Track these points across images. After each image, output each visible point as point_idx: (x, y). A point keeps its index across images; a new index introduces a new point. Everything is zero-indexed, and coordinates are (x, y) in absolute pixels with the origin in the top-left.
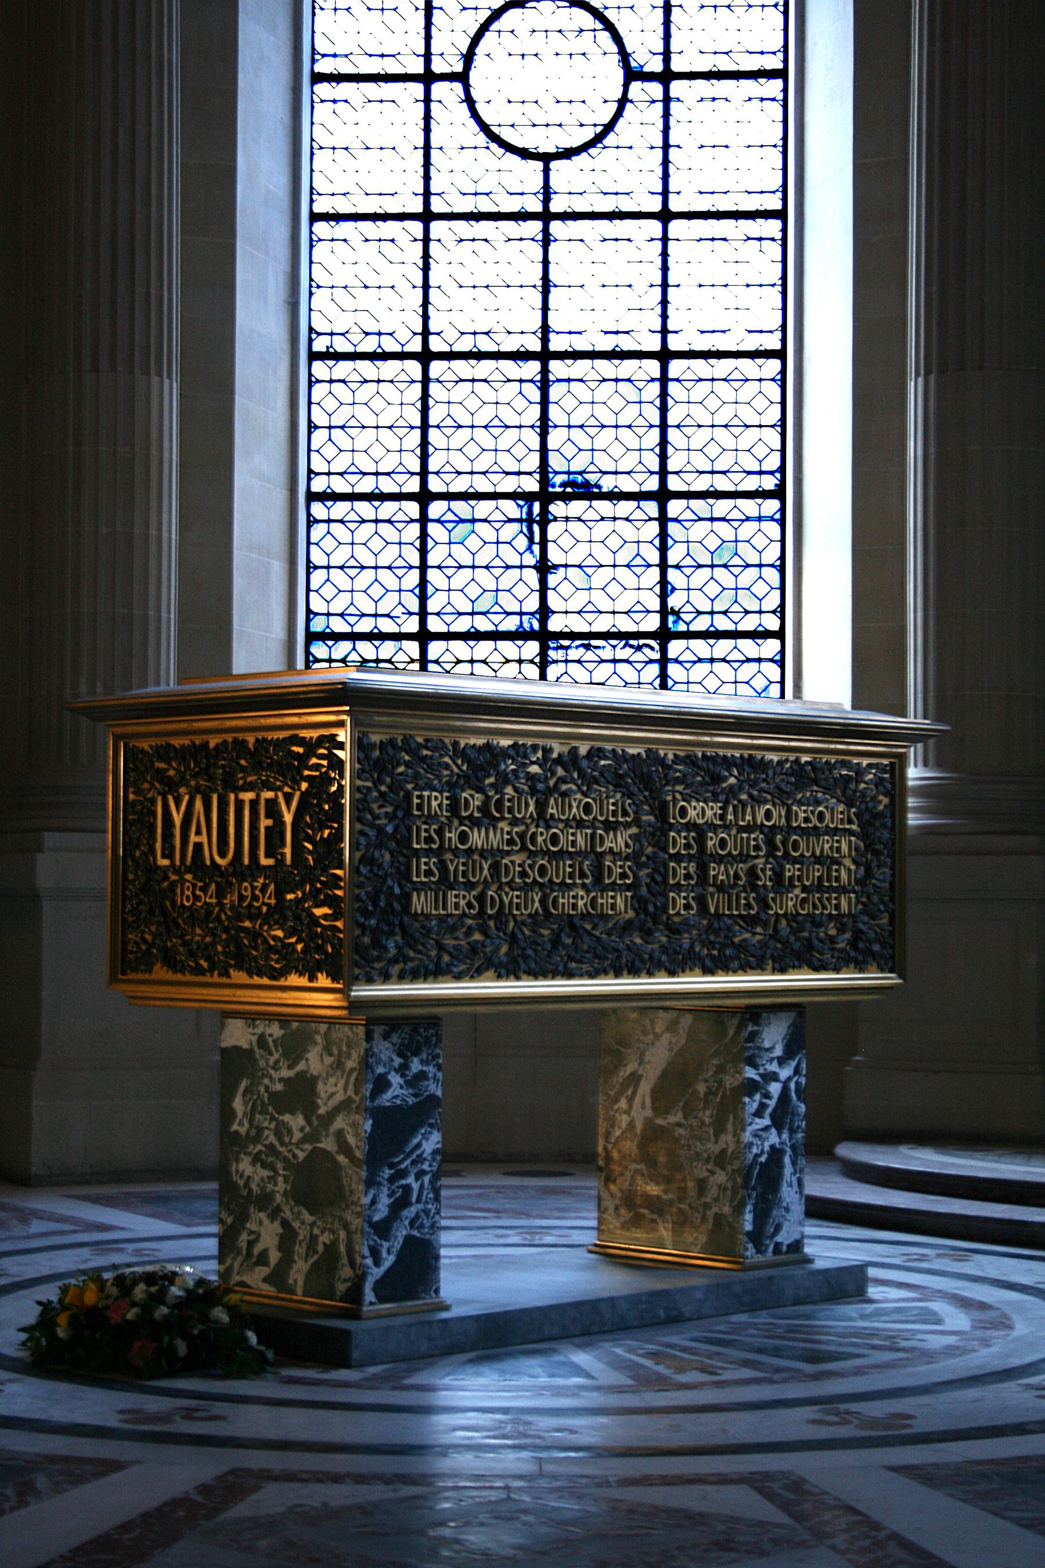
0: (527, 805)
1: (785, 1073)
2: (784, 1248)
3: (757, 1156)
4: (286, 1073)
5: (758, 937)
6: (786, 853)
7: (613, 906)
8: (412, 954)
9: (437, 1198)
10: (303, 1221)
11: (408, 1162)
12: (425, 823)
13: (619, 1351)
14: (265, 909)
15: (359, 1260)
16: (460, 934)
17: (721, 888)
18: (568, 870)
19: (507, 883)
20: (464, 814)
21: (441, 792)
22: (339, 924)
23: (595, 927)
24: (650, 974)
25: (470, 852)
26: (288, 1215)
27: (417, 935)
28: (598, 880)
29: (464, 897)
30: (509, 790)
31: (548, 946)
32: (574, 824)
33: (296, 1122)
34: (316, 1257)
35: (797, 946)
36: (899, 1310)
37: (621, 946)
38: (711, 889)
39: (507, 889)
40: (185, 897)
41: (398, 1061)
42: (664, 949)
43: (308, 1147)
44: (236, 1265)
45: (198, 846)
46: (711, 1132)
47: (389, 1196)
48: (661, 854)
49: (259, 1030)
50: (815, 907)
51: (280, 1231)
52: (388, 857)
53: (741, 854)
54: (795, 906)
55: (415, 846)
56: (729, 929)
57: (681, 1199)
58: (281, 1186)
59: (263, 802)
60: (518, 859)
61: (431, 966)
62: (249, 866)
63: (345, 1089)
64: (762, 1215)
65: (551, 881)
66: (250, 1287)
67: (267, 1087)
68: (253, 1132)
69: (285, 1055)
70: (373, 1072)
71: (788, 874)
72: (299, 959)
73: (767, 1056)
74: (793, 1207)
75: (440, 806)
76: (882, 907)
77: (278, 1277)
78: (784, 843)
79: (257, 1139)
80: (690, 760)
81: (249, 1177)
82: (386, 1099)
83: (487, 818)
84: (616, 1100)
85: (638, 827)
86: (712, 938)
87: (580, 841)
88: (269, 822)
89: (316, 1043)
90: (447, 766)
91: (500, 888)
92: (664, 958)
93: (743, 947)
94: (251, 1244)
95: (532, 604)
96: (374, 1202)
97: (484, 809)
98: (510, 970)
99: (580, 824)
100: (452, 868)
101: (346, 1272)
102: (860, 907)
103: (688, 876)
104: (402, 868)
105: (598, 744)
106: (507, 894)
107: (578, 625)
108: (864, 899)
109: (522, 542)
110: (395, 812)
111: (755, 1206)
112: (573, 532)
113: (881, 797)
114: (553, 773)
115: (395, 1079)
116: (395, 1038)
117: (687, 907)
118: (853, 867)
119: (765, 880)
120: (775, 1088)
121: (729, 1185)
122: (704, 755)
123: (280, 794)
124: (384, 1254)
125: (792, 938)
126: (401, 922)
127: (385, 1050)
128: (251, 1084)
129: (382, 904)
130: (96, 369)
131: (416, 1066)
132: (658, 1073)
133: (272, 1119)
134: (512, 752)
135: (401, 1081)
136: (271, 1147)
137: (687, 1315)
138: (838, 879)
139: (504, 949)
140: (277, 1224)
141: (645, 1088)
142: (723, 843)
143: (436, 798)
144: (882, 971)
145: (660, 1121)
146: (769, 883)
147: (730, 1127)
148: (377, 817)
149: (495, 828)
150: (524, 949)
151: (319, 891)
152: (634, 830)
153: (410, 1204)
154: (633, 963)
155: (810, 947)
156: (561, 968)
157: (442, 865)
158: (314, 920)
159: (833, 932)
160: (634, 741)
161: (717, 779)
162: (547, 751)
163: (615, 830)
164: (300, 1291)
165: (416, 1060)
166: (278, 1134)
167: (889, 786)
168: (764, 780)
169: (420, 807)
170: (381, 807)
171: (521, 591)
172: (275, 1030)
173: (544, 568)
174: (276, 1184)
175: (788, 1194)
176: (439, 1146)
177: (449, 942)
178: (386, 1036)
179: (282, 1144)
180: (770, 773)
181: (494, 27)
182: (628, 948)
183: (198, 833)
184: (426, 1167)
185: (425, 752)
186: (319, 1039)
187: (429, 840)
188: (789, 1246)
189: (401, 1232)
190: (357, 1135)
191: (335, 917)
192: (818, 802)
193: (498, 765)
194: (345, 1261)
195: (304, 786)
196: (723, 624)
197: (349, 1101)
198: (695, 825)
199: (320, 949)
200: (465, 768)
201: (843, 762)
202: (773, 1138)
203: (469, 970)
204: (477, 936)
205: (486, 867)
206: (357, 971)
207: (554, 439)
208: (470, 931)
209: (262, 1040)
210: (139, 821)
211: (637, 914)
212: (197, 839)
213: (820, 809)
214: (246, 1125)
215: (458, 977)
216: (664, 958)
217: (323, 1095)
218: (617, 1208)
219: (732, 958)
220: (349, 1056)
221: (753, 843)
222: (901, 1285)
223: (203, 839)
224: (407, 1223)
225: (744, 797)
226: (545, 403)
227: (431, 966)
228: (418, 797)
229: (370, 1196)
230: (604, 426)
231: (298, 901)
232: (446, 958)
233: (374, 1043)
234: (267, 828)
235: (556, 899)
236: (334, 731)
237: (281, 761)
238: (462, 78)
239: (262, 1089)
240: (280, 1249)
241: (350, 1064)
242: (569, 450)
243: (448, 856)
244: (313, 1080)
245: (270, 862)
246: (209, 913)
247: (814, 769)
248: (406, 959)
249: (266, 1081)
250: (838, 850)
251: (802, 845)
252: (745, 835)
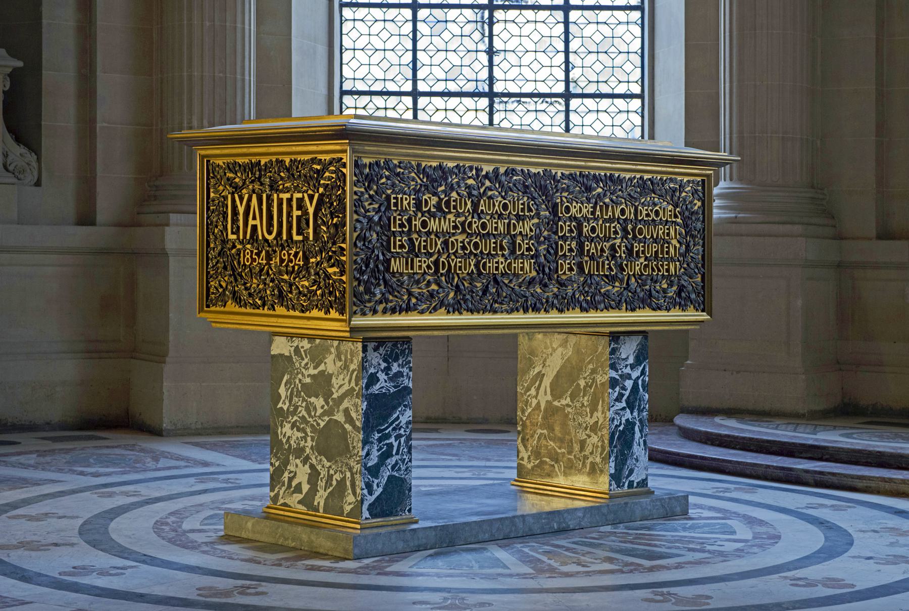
0: (466, 204)
1: (635, 374)
2: (635, 485)
3: (616, 426)
5: (616, 289)
6: (635, 237)
7: (522, 269)
8: (391, 297)
9: (410, 452)
10: (324, 465)
11: (390, 429)
12: (399, 215)
13: (526, 550)
14: (296, 268)
15: (358, 491)
16: (423, 285)
17: (592, 258)
18: (493, 245)
19: (454, 254)
20: (424, 209)
21: (409, 196)
22: (344, 278)
23: (511, 281)
24: (546, 311)
25: (428, 233)
26: (314, 461)
27: (395, 286)
28: (513, 252)
29: (425, 262)
30: (454, 194)
31: (480, 293)
32: (496, 217)
33: (319, 402)
34: (331, 488)
35: (641, 295)
36: (705, 525)
37: (528, 294)
38: (586, 258)
39: (453, 257)
40: (246, 259)
41: (384, 365)
42: (556, 296)
46: (588, 410)
47: (378, 451)
48: (553, 236)
50: (653, 270)
51: (309, 471)
52: (375, 236)
53: (605, 236)
54: (640, 269)
55: (393, 229)
56: (597, 284)
57: (570, 453)
58: (309, 443)
59: (294, 200)
60: (460, 238)
61: (404, 306)
62: (287, 240)
64: (621, 462)
65: (481, 252)
66: (290, 507)
70: (367, 372)
71: (635, 250)
72: (318, 300)
73: (623, 364)
74: (640, 459)
75: (409, 204)
76: (696, 271)
77: (308, 501)
78: (633, 230)
80: (571, 177)
82: (375, 389)
83: (441, 210)
84: (528, 389)
85: (539, 218)
86: (586, 289)
87: (501, 228)
88: (299, 213)
89: (331, 353)
90: (414, 179)
91: (448, 256)
92: (556, 301)
93: (606, 295)
96: (368, 454)
97: (438, 206)
98: (455, 308)
99: (500, 216)
100: (417, 244)
101: (351, 498)
102: (682, 270)
103: (571, 250)
104: (385, 243)
105: (511, 166)
106: (453, 260)
108: (685, 266)
110: (379, 207)
111: (616, 457)
113: (696, 201)
114: (483, 184)
115: (382, 376)
116: (381, 350)
117: (571, 269)
118: (678, 245)
119: (622, 253)
120: (629, 384)
121: (600, 444)
122: (581, 173)
123: (305, 195)
124: (375, 487)
125: (639, 290)
126: (384, 277)
127: (375, 358)
129: (371, 266)
131: (395, 368)
132: (555, 373)
134: (456, 171)
135: (386, 377)
137: (571, 527)
138: (668, 253)
139: (452, 295)
140: (307, 466)
141: (547, 382)
142: (593, 230)
143: (406, 199)
144: (697, 310)
145: (556, 403)
146: (623, 255)
147: (600, 407)
148: (368, 211)
149: (445, 218)
150: (464, 295)
151: (330, 258)
152: (536, 221)
153: (392, 456)
154: (535, 304)
155: (650, 296)
156: (488, 307)
157: (411, 240)
158: (328, 276)
159: (665, 286)
160: (535, 166)
161: (589, 189)
162: (478, 170)
163: (523, 220)
164: (321, 510)
165: (395, 365)
167: (701, 195)
168: (620, 190)
169: (396, 205)
170: (370, 204)
174: (306, 442)
175: (638, 450)
176: (411, 418)
177: (416, 290)
178: (376, 349)
180: (624, 185)
182: (532, 295)
184: (402, 432)
185: (399, 170)
186: (333, 350)
187: (402, 225)
188: (638, 483)
189: (386, 473)
190: (357, 411)
191: (342, 273)
192: (655, 204)
193: (446, 179)
194: (350, 491)
195: (321, 190)
197: (353, 389)
198: (575, 218)
199: (330, 293)
200: (425, 180)
201: (671, 180)
202: (628, 415)
203: (428, 308)
204: (434, 287)
205: (439, 243)
206: (355, 308)
208: (429, 284)
210: (215, 212)
211: (538, 274)
213: (657, 208)
215: (422, 312)
216: (556, 301)
217: (335, 385)
218: (529, 458)
219: (599, 303)
220: (352, 361)
221: (613, 229)
222: (711, 508)
224: (389, 467)
225: (607, 200)
227: (404, 306)
228: (394, 198)
229: (366, 451)
231: (317, 264)
232: (414, 300)
233: (368, 354)
235: (485, 263)
236: (340, 155)
237: (306, 174)
240: (308, 483)
243: (415, 236)
245: (300, 238)
246: (261, 270)
247: (652, 183)
248: (387, 301)
250: (668, 234)
251: (645, 231)
252: (608, 225)
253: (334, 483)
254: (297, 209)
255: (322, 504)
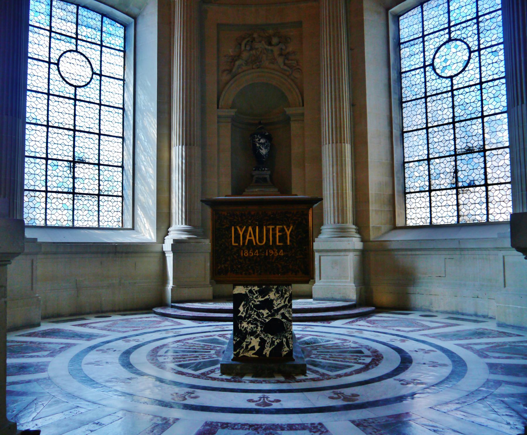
4: (260, 299)
10: (269, 338)
26: (262, 336)
33: (265, 312)
43: (270, 318)
44: (241, 352)
45: (250, 241)
49: (250, 288)
63: (284, 302)
67: (253, 304)
68: (248, 315)
69: (260, 294)
79: (248, 318)
81: (246, 328)
89: (272, 291)
94: (247, 346)
95: (71, 186)
101: (286, 349)
107: (81, 191)
109: (69, 172)
112: (80, 169)
128: (247, 303)
130: (7, 115)
133: (255, 311)
136: (255, 319)
166: (258, 315)
171: (68, 183)
172: (256, 288)
173: (74, 178)
174: (257, 328)
179: (259, 317)
181: (64, 55)
183: (250, 236)
186: (273, 290)
194: (286, 346)
196: (110, 193)
197: (287, 305)
207: (76, 149)
209: (251, 291)
212: (250, 238)
214: (245, 314)
223: (253, 238)
226: (74, 141)
230: (86, 147)
234: (279, 236)
238: (57, 64)
239: (251, 304)
240: (259, 345)
241: (286, 296)
242: (79, 152)
244: (272, 300)
245: (281, 244)
249: (253, 302)
253: (276, 344)
254: (279, 232)
255: (268, 353)
